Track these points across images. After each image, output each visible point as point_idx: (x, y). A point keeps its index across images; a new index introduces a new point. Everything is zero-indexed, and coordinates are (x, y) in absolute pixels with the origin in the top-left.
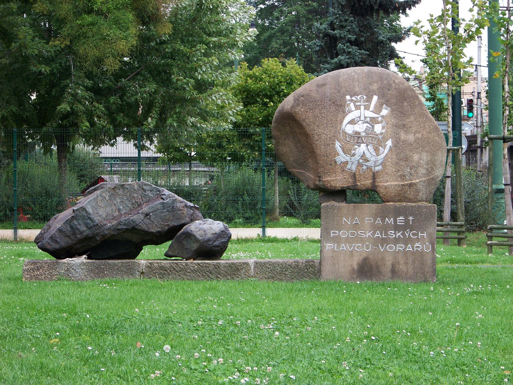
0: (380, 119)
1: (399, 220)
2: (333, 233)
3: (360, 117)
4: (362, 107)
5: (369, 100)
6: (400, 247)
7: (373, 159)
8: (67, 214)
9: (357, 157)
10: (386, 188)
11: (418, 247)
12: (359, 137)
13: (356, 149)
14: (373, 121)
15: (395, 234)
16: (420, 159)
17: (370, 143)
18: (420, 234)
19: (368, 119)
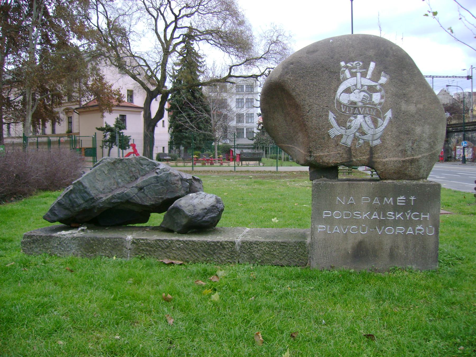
0: (378, 87)
1: (399, 200)
2: (326, 214)
3: (356, 85)
4: (359, 75)
5: (366, 66)
6: (400, 229)
7: (370, 132)
9: (353, 130)
10: (384, 164)
11: (420, 230)
12: (355, 108)
13: (352, 120)
14: (371, 89)
16: (423, 132)
17: (367, 114)
19: (366, 88)
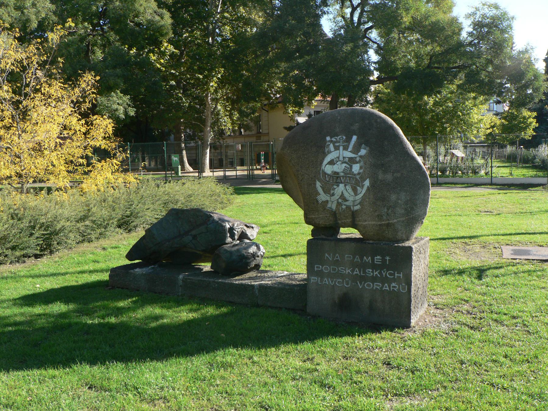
0: (358, 159)
1: (376, 259)
2: (317, 267)
3: (338, 158)
4: (341, 148)
5: (349, 140)
6: (377, 285)
7: (351, 199)
8: (216, 174)
9: (336, 197)
11: (395, 287)
12: (338, 177)
13: (335, 188)
14: (352, 161)
15: (373, 272)
16: (398, 199)
17: (348, 183)
18: (396, 275)
19: (347, 160)
